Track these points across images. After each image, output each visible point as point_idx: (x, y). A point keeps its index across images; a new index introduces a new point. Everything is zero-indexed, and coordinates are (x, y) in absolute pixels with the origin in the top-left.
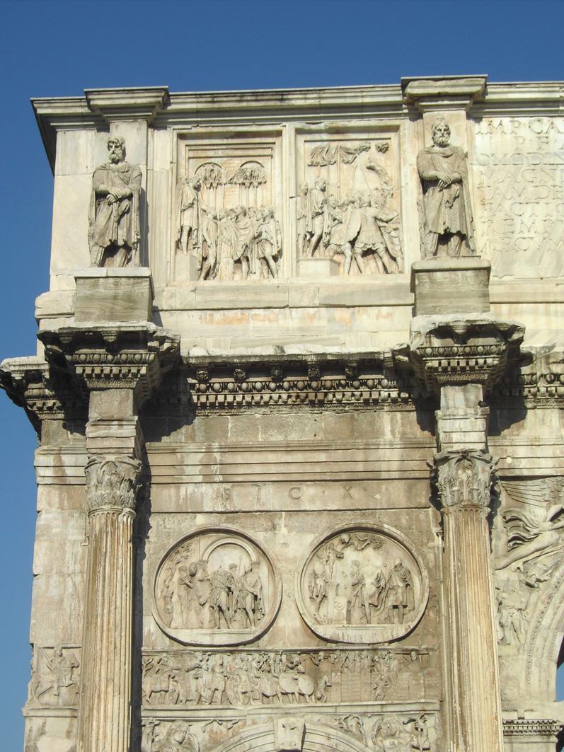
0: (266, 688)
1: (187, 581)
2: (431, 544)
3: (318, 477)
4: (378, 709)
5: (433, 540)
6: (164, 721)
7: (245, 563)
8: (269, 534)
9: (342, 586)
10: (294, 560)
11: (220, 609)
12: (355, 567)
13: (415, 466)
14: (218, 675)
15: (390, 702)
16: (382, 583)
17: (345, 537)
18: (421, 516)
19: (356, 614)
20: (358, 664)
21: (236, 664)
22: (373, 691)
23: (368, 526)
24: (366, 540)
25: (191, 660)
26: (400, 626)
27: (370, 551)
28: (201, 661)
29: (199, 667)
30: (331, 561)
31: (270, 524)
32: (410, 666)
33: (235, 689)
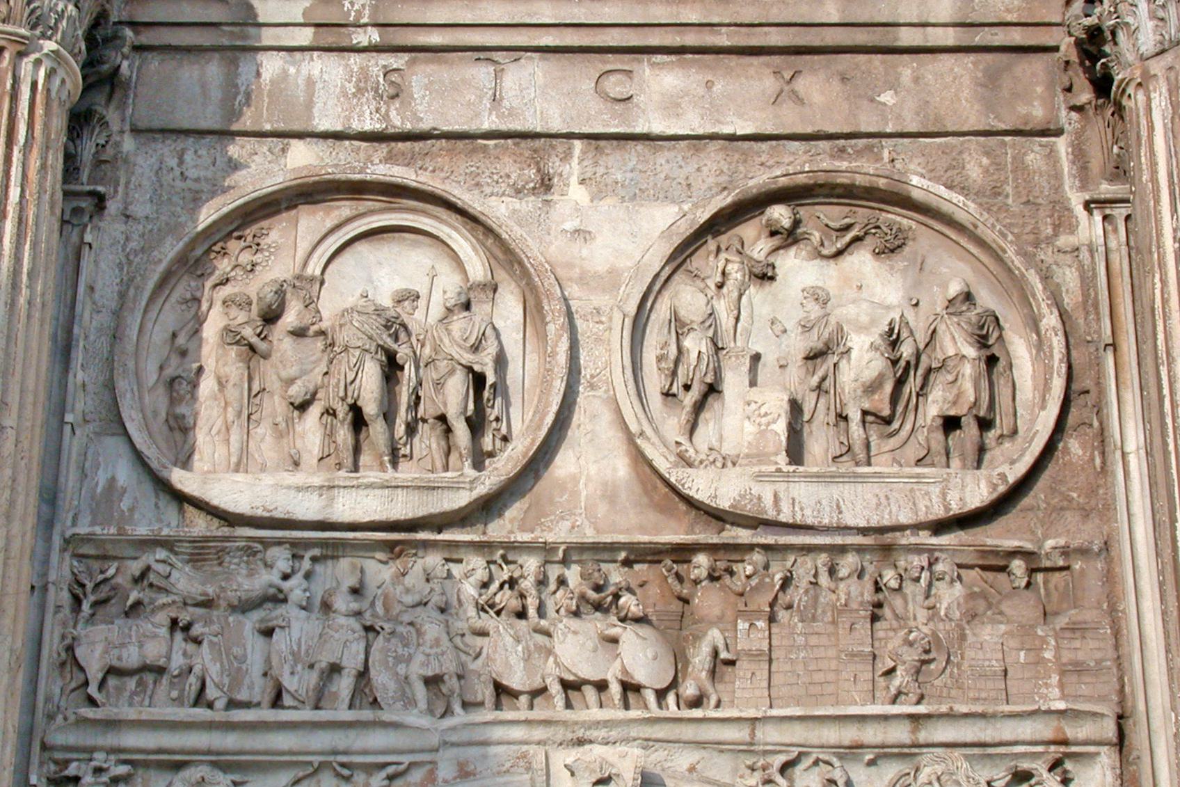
0: (508, 665)
1: (248, 332)
2: (1064, 241)
3: (691, 39)
4: (899, 734)
5: (1072, 229)
6: (146, 765)
7: (448, 285)
8: (529, 204)
9: (769, 359)
10: (611, 281)
11: (358, 421)
12: (815, 310)
13: (1008, 11)
14: (342, 620)
15: (944, 709)
16: (906, 351)
17: (780, 214)
18: (1030, 157)
19: (819, 444)
20: (825, 598)
21: (408, 591)
22: (881, 682)
23: (860, 180)
24: (848, 228)
25: (251, 574)
26: (970, 476)
27: (862, 261)
28: (286, 577)
29: (278, 598)
30: (731, 285)
31: (532, 172)
32: (1005, 607)
33: (401, 669)
